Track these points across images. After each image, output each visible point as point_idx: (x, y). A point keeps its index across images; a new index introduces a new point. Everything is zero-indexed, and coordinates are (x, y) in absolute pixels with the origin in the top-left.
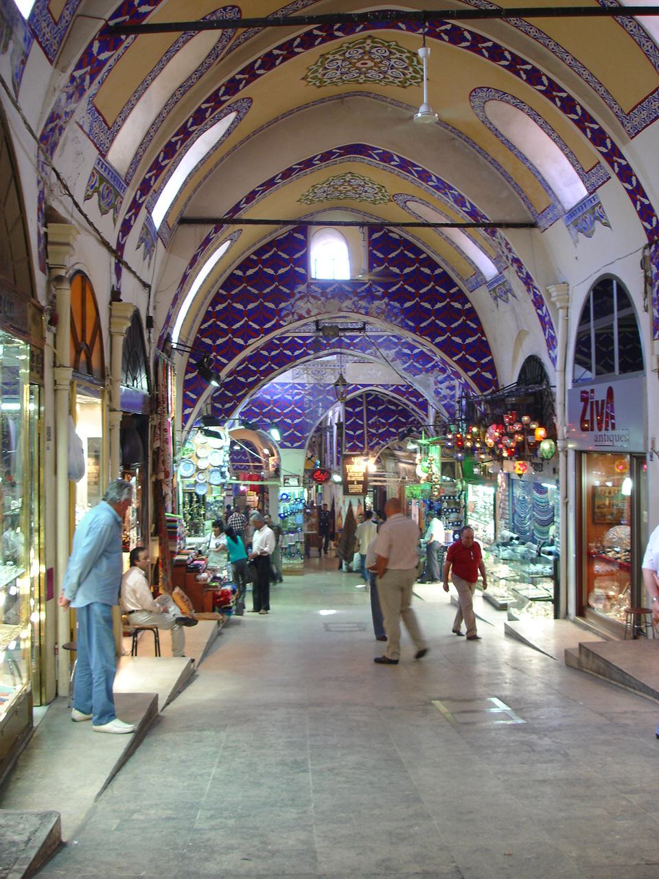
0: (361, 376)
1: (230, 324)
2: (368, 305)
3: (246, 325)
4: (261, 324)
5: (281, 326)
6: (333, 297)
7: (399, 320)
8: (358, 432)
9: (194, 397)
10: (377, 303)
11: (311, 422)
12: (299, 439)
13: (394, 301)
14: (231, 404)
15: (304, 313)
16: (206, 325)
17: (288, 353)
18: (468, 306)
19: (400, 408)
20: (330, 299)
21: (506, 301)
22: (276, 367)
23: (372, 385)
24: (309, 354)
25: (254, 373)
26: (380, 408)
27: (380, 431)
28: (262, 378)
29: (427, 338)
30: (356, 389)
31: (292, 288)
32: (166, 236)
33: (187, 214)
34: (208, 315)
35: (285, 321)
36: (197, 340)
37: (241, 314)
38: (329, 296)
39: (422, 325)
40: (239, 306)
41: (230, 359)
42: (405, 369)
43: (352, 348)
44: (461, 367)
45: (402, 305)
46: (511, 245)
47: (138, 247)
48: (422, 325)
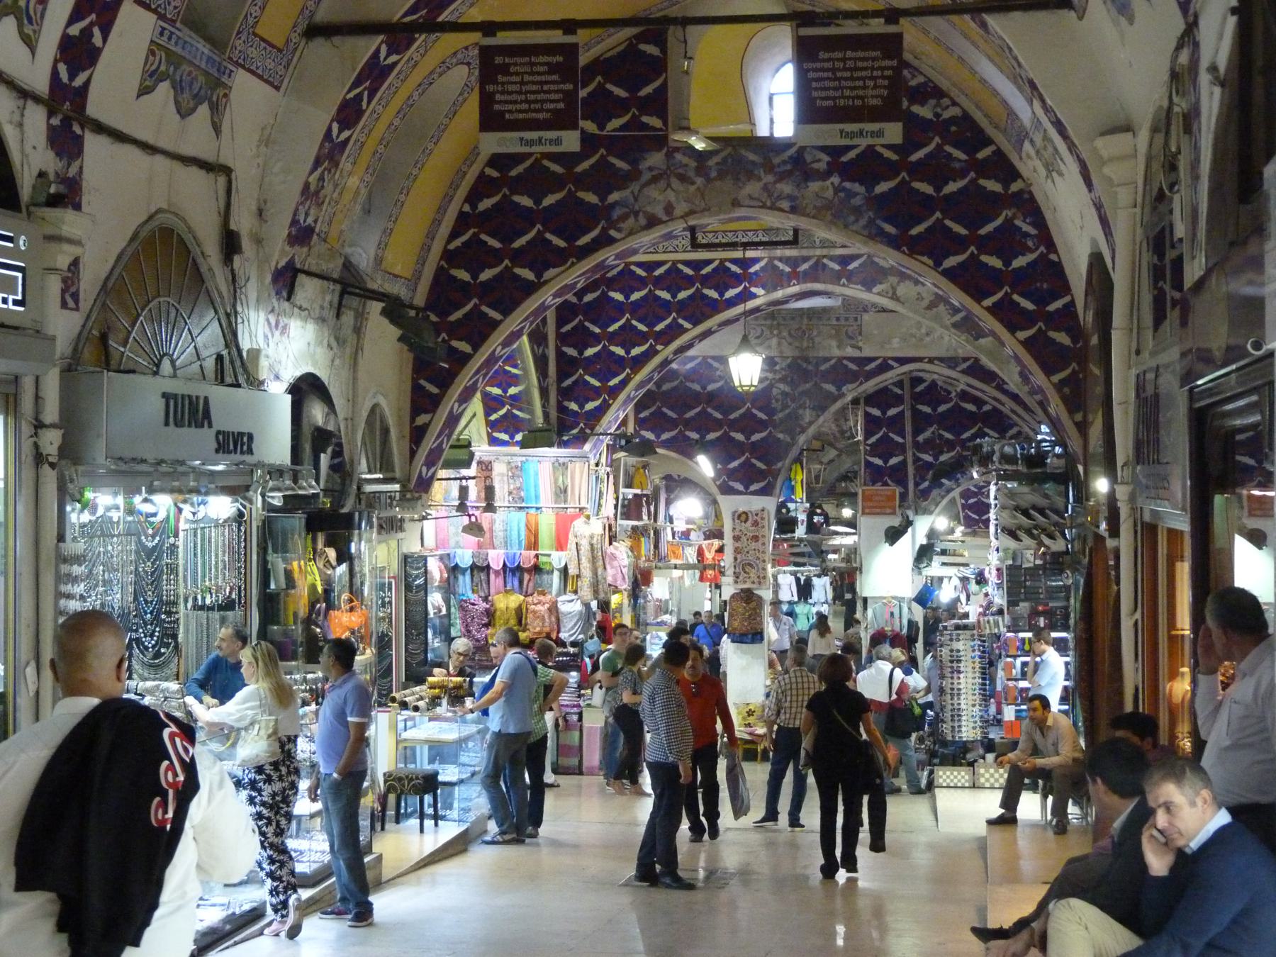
0: (896, 341)
1: (507, 239)
2: (796, 193)
3: (540, 240)
4: (571, 239)
5: (612, 241)
6: (721, 176)
7: (863, 222)
8: (893, 461)
9: (435, 390)
10: (814, 186)
11: (788, 439)
12: (761, 475)
13: (853, 180)
14: (597, 403)
15: (659, 211)
16: (457, 243)
17: (713, 294)
18: (1015, 187)
19: (986, 408)
20: (715, 179)
21: (1061, 174)
22: (687, 325)
23: (920, 360)
24: (755, 296)
25: (643, 337)
26: (943, 408)
27: (943, 458)
28: (659, 347)
29: (925, 259)
30: (884, 367)
31: (634, 162)
32: (270, 64)
33: (322, 16)
34: (463, 222)
35: (619, 230)
36: (441, 279)
37: (529, 218)
38: (714, 174)
39: (914, 232)
40: (526, 201)
41: (506, 312)
42: (955, 325)
43: (844, 281)
44: (1001, 321)
45: (870, 188)
46: (1016, 51)
47: (144, 91)
48: (914, 232)
